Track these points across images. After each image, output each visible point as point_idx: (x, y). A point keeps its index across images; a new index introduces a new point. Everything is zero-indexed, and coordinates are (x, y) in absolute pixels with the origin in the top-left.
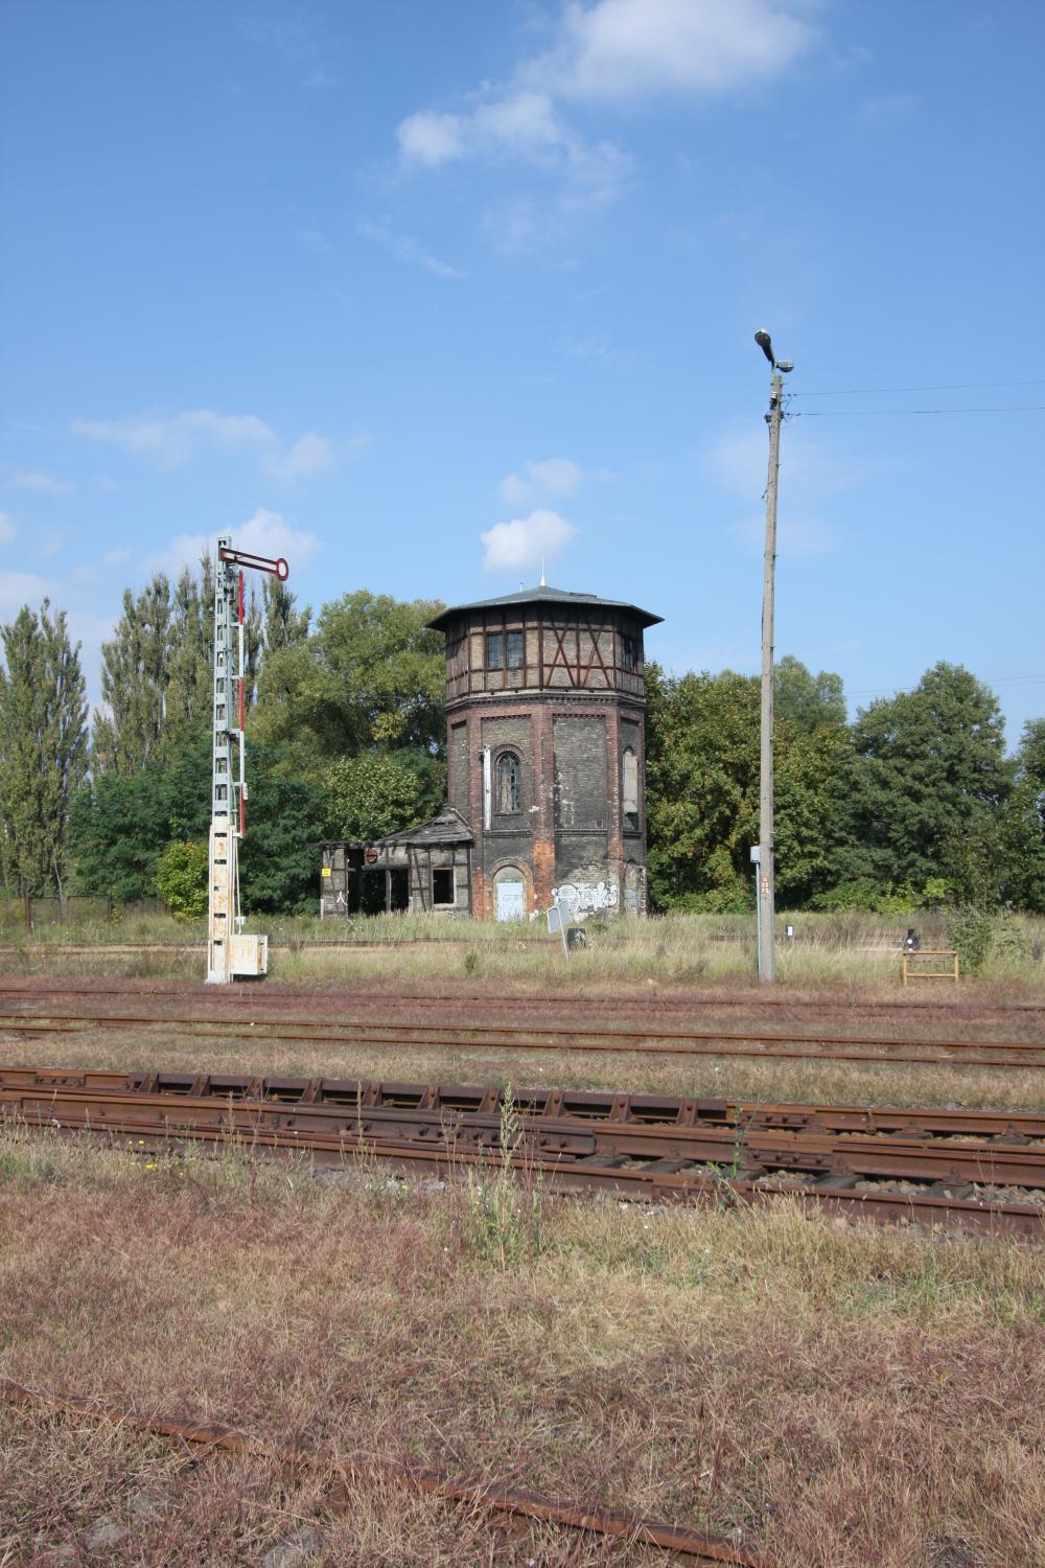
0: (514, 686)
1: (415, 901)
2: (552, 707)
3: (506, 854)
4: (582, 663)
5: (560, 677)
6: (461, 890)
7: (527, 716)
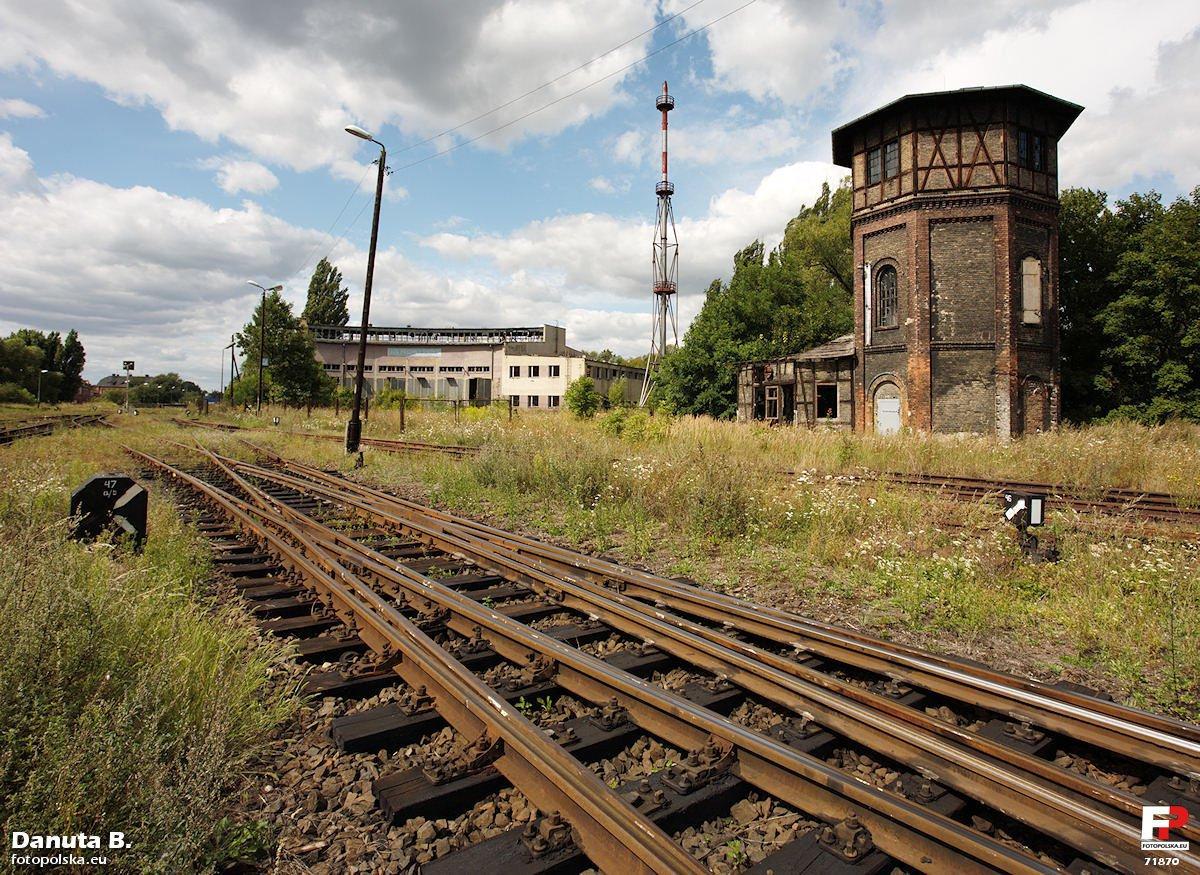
0: (891, 196)
1: (799, 415)
2: (929, 213)
3: (884, 369)
4: (964, 162)
5: (938, 179)
6: (844, 405)
7: (902, 226)
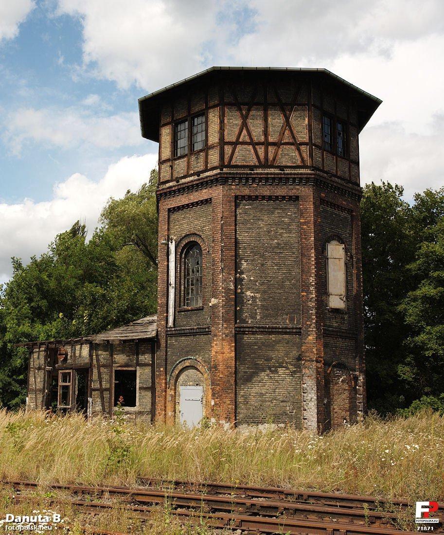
0: (197, 170)
1: (94, 403)
2: (236, 189)
3: (187, 353)
4: (271, 140)
5: (244, 155)
6: (144, 393)
7: (208, 201)
